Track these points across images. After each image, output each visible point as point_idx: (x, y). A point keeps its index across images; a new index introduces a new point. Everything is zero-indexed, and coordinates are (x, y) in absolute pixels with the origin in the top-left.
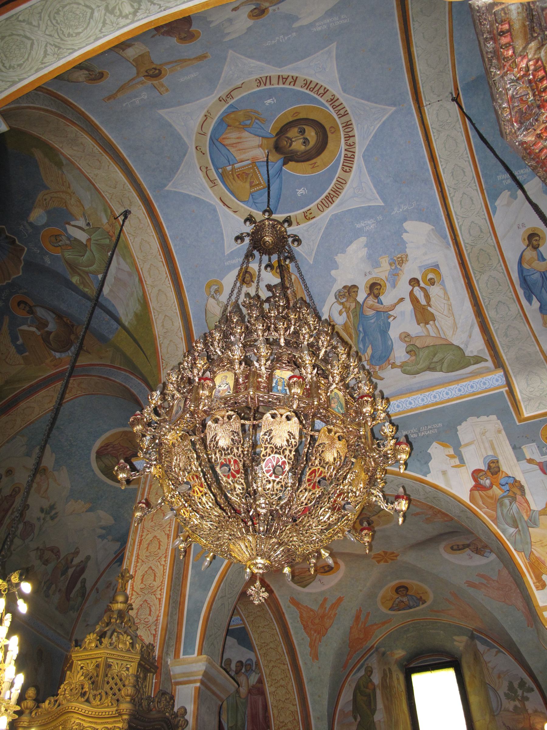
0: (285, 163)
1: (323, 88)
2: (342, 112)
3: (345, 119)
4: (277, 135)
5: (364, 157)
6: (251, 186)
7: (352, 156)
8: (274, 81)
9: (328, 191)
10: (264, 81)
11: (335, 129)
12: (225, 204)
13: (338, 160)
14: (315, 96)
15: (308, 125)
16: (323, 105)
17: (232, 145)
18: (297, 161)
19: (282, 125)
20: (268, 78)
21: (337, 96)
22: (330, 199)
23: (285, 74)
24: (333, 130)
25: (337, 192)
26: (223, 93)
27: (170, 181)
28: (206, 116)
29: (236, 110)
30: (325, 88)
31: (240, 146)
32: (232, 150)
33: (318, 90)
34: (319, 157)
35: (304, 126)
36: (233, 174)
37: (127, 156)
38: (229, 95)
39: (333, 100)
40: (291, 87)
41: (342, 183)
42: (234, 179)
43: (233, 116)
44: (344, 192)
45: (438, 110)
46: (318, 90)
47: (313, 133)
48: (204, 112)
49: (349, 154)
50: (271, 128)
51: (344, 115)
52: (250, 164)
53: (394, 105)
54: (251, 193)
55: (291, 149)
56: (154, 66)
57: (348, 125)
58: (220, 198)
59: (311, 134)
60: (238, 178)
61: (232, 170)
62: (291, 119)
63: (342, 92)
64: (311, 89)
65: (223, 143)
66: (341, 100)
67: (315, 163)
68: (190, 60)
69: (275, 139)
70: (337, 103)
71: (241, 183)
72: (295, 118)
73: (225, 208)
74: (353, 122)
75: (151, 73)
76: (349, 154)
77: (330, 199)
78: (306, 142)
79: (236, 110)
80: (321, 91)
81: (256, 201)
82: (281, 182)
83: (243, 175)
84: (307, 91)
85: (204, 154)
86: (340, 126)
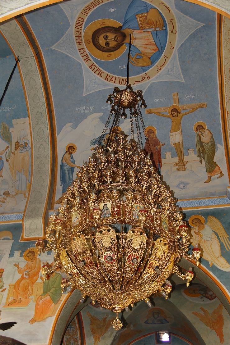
0: (121, 27)
1: (92, 69)
2: (82, 51)
3: (81, 47)
4: (123, 44)
5: (69, 25)
6: (146, 17)
7: (77, 26)
8: (118, 80)
9: (94, 9)
10: (123, 82)
11: (87, 42)
12: (168, 8)
13: (86, 24)
14: (96, 65)
15: (103, 47)
16: (93, 58)
17: (151, 44)
18: (113, 27)
19: (118, 50)
20: (120, 83)
21: (84, 62)
22: (93, 4)
23: (111, 83)
24: (89, 42)
25: (88, 8)
26: (146, 81)
27: (199, 29)
28: (160, 69)
29: (143, 68)
30: (91, 69)
31: (147, 42)
32: (152, 41)
33: (95, 68)
34: (98, 28)
35: (106, 47)
36: (157, 25)
37: (216, 57)
38: (143, 78)
39: (87, 60)
40: (109, 74)
41: (85, 12)
42: (157, 22)
43: (145, 64)
44: (84, 7)
45: (26, 53)
46: (95, 68)
47: (101, 42)
48: (160, 72)
49: (79, 27)
50: (125, 49)
51: (81, 49)
52: (143, 29)
53: (51, 50)
54: (148, 12)
55: (116, 35)
56: (173, 118)
57: (79, 43)
58: (170, 12)
59: (102, 41)
60: (153, 22)
61: (156, 27)
62: (112, 53)
63: (82, 64)
64: (98, 70)
65: (156, 47)
66: (82, 59)
67: (101, 25)
68: (155, 113)
69: (125, 42)
70: (85, 57)
71: (152, 19)
72: (110, 53)
73: (168, 6)
74: (76, 44)
75: (176, 114)
76: (79, 27)
77: (93, 4)
78: (106, 38)
79: (143, 68)
80: (93, 67)
81: (146, 8)
82: (126, 17)
83: (150, 23)
84: (101, 69)
85: (170, 42)
86: (84, 43)
